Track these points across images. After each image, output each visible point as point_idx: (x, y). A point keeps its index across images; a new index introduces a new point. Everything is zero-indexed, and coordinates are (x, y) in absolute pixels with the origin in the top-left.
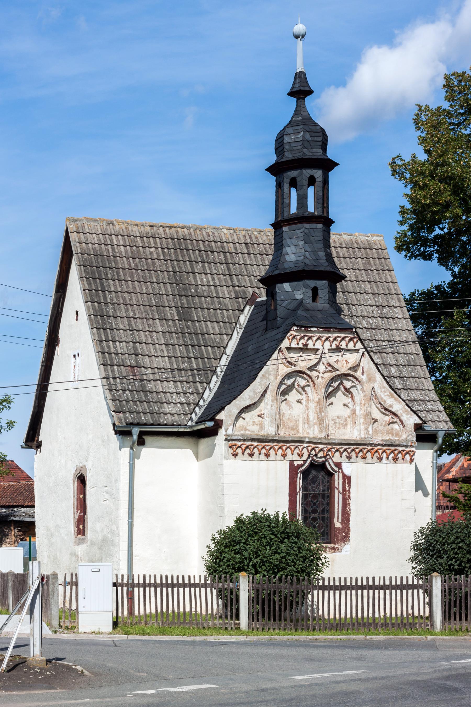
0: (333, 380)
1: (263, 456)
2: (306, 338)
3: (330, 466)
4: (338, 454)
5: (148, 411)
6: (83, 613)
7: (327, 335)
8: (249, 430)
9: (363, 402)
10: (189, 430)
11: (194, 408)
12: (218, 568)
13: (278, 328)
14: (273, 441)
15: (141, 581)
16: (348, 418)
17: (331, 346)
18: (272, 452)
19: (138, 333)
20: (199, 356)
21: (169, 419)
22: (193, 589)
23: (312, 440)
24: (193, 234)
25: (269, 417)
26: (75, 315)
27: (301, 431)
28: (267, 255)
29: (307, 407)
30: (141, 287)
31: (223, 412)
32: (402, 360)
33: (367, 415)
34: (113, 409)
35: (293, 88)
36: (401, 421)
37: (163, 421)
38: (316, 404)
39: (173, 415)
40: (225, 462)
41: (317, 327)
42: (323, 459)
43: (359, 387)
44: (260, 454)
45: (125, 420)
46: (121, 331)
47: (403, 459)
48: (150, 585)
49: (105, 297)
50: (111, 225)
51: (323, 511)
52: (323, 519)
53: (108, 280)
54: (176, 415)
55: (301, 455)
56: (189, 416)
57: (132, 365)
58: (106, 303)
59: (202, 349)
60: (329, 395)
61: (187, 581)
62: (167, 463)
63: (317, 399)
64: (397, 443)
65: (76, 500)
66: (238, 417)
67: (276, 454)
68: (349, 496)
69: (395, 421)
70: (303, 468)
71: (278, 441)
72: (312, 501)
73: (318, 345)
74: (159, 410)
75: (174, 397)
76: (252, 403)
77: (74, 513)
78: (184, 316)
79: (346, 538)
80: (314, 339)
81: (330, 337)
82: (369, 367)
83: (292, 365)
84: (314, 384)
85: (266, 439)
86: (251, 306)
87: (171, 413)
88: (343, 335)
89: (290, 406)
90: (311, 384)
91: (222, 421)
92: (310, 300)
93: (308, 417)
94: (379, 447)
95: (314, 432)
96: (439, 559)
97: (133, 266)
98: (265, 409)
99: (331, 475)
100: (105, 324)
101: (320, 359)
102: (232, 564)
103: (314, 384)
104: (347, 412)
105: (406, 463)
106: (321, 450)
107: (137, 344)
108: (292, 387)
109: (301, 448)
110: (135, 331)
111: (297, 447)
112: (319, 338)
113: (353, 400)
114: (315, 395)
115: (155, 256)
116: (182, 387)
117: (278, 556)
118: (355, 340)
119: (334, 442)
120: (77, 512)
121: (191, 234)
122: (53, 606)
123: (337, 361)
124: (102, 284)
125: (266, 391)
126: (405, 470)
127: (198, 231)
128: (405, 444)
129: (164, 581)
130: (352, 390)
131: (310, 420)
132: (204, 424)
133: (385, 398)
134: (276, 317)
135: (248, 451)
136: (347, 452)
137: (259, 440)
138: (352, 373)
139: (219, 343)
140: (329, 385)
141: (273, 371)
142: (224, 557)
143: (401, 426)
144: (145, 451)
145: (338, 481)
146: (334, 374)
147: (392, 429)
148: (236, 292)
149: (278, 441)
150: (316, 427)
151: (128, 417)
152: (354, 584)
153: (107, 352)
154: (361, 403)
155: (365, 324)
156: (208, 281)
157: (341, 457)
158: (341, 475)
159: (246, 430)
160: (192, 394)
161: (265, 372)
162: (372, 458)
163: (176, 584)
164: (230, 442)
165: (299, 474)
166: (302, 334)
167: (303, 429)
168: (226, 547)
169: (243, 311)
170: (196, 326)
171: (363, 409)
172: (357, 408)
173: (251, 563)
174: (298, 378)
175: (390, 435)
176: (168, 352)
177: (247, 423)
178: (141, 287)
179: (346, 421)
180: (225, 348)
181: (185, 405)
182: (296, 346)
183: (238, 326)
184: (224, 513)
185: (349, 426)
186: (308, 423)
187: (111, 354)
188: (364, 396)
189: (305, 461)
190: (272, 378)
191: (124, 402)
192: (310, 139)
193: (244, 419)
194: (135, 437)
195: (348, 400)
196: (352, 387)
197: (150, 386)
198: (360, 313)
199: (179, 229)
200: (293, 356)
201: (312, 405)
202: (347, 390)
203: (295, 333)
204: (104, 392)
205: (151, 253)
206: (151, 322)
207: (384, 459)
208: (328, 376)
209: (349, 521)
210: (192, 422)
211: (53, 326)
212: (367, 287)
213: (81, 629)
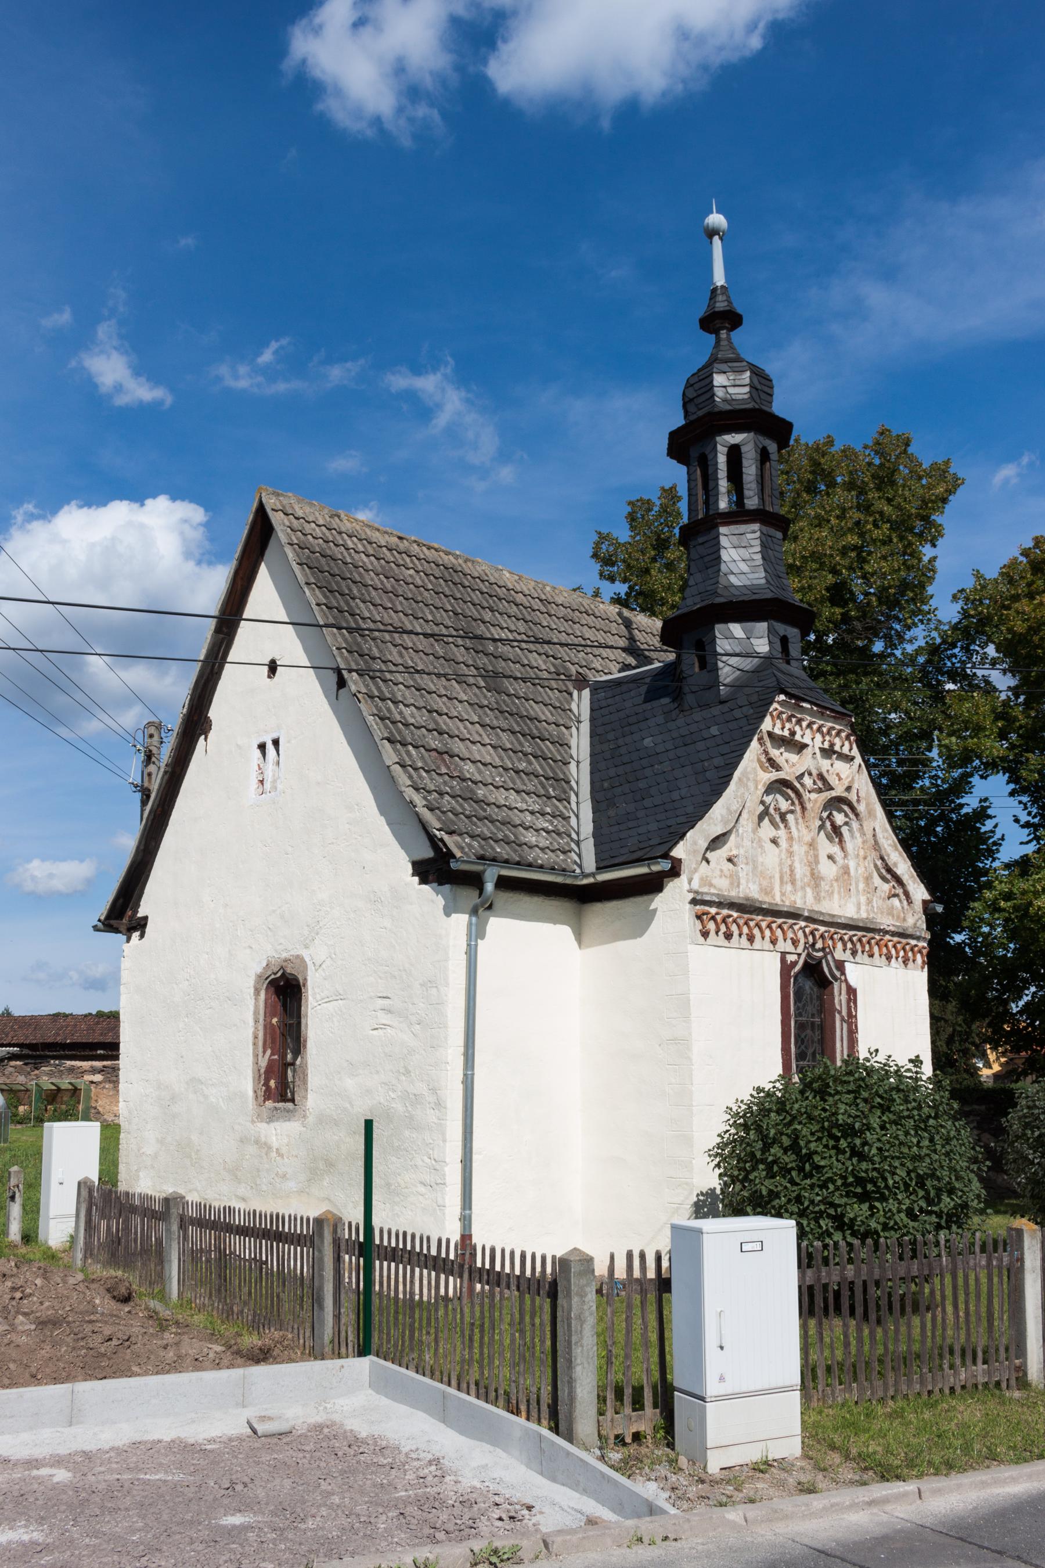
6: (719, 1398)
9: (862, 853)
21: (543, 858)
25: (747, 864)
31: (681, 843)
40: (691, 948)
41: (811, 703)
42: (820, 954)
43: (855, 825)
65: (261, 1028)
68: (856, 1026)
77: (256, 1056)
83: (773, 767)
85: (751, 906)
90: (798, 808)
94: (888, 937)
103: (803, 808)
113: (843, 849)
120: (264, 1052)
122: (578, 1369)
130: (845, 830)
131: (798, 876)
132: (649, 866)
143: (905, 903)
144: (496, 925)
145: (840, 999)
147: (892, 907)
150: (809, 890)
158: (844, 985)
159: (711, 885)
161: (742, 773)
164: (698, 907)
167: (783, 894)
171: (862, 865)
172: (852, 864)
179: (832, 886)
185: (836, 896)
186: (793, 882)
195: (835, 849)
201: (800, 850)
211: (200, 697)
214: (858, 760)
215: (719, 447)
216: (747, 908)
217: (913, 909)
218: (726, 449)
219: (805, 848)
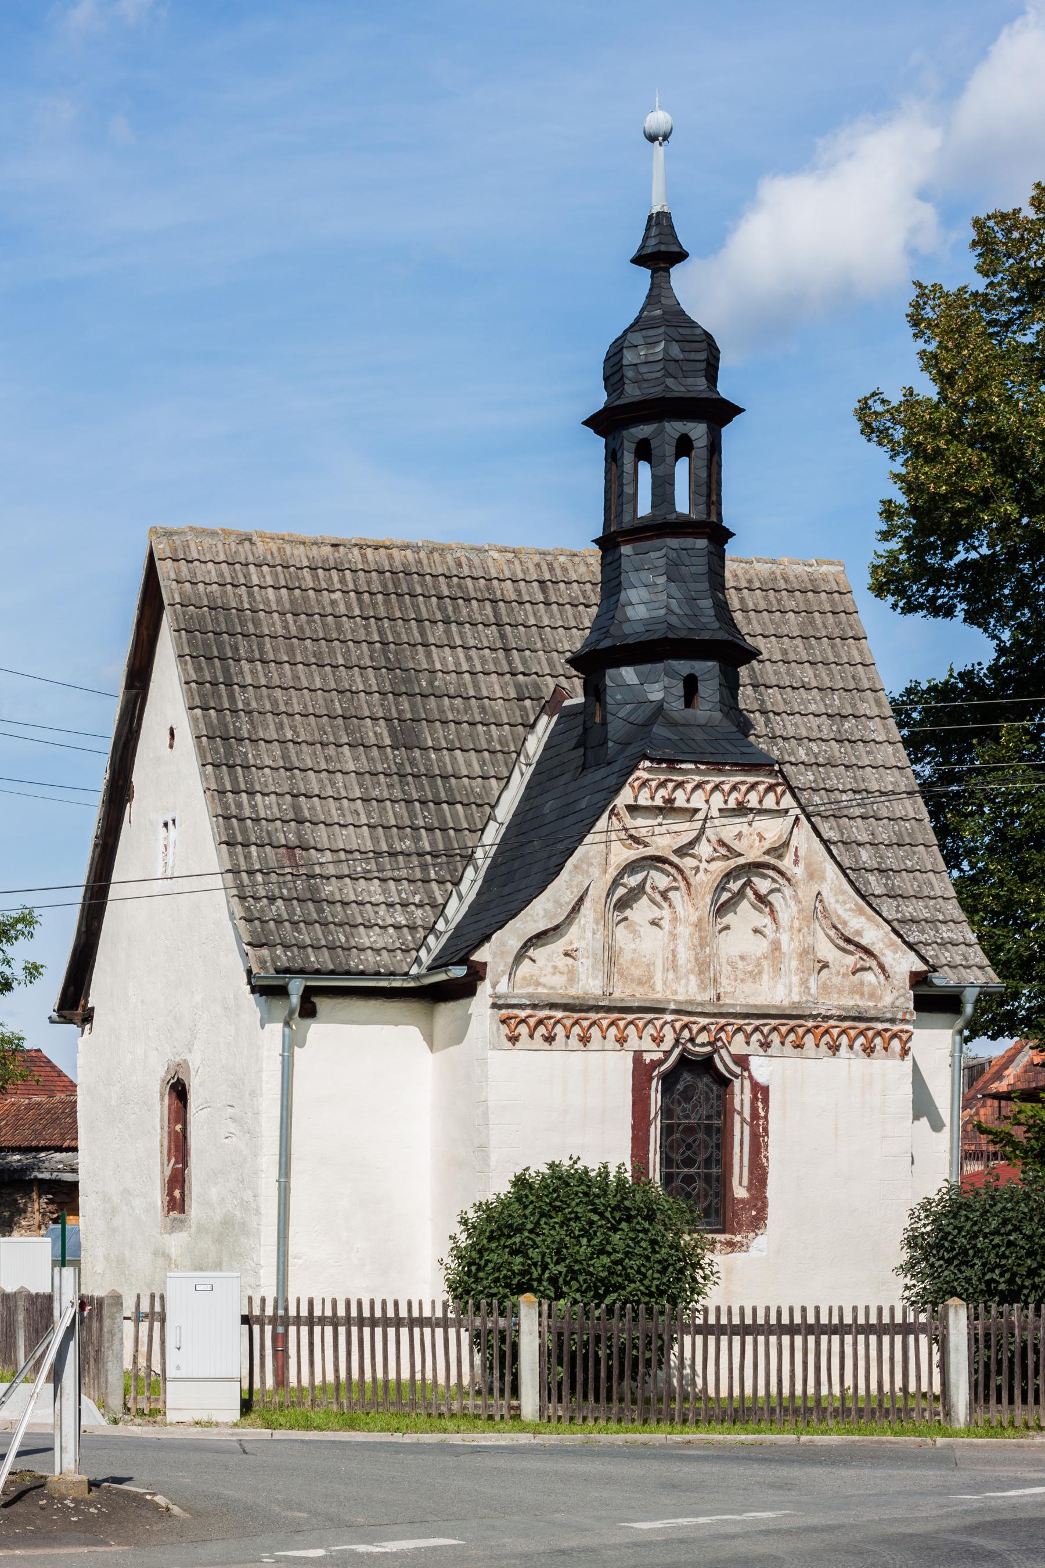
0: (728, 876)
1: (574, 1042)
2: (670, 785)
3: (723, 1062)
4: (740, 1037)
5: (323, 943)
6: (176, 1380)
7: (718, 780)
8: (544, 986)
9: (796, 924)
10: (412, 984)
11: (425, 938)
12: (474, 1286)
13: (609, 764)
14: (597, 1009)
15: (304, 1312)
16: (764, 960)
17: (726, 802)
18: (595, 1032)
19: (303, 774)
20: (436, 825)
22: (417, 1331)
23: (683, 1007)
24: (425, 562)
25: (588, 957)
26: (168, 737)
27: (659, 986)
28: (587, 606)
29: (673, 936)
30: (310, 676)
31: (487, 945)
32: (884, 832)
33: (806, 952)
34: (247, 938)
37: (357, 966)
38: (691, 929)
39: (377, 951)
40: (491, 1054)
41: (695, 762)
42: (709, 1049)
43: (788, 891)
44: (568, 1037)
45: (273, 962)
46: (267, 771)
47: (886, 1049)
48: (323, 1321)
49: (232, 697)
50: (247, 543)
51: (708, 1163)
52: (708, 1178)
53: (239, 661)
54: (384, 953)
55: (658, 1040)
56: (414, 953)
57: (291, 844)
58: (234, 712)
59: (442, 810)
60: (721, 910)
62: (365, 1055)
63: (694, 919)
64: (872, 1013)
66: (520, 956)
67: (605, 1038)
68: (766, 1129)
69: (868, 965)
70: (662, 1068)
71: (609, 1009)
72: (684, 1141)
73: (698, 801)
74: (347, 941)
75: (381, 913)
76: (550, 926)
78: (405, 737)
79: (758, 1222)
80: (689, 787)
81: (723, 783)
82: (809, 849)
83: (639, 843)
84: (688, 884)
85: (581, 1005)
86: (551, 716)
87: (375, 948)
88: (752, 779)
89: (634, 932)
90: (682, 884)
91: (485, 964)
92: (680, 704)
93: (674, 956)
94: (832, 1023)
95: (687, 990)
97: (293, 630)
98: (579, 940)
99: (724, 1083)
100: (232, 755)
101: (702, 830)
102: (505, 1277)
103: (688, 884)
104: (762, 946)
105: (894, 1058)
106: (704, 1028)
107: (302, 799)
109: (658, 1023)
110: (296, 771)
111: (650, 1022)
112: (698, 786)
113: (774, 920)
114: (689, 908)
115: (342, 609)
116: (399, 892)
117: (605, 1260)
118: (779, 789)
119: (731, 1010)
121: (420, 562)
122: (110, 1364)
123: (739, 835)
124: (226, 670)
125: (581, 900)
126: (890, 1074)
127: (436, 555)
128: (889, 1015)
129: (354, 1313)
131: (680, 963)
132: (446, 972)
133: (845, 916)
135: (542, 1030)
136: (762, 1032)
137: (566, 1007)
138: (773, 861)
139: (480, 796)
140: (721, 888)
141: (598, 857)
142: (488, 1262)
143: (882, 977)
145: (741, 1097)
146: (732, 863)
147: (862, 983)
148: (518, 687)
149: (609, 1009)
150: (693, 978)
151: (279, 957)
152: (773, 1321)
153: (235, 817)
154: (792, 927)
155: (802, 754)
156: (457, 663)
157: (748, 1043)
158: (747, 1083)
159: (538, 984)
161: (580, 860)
162: (817, 1046)
163: (379, 1319)
164: (503, 1011)
165: (654, 1082)
166: (662, 778)
167: (665, 983)
168: (491, 1239)
169: (533, 726)
170: (429, 759)
171: (796, 939)
172: (784, 938)
173: (547, 1275)
174: (653, 873)
175: (857, 997)
176: (369, 816)
177: (541, 969)
178: (310, 676)
179: (759, 964)
180: (493, 807)
181: (405, 930)
182: (649, 803)
183: (522, 759)
184: (488, 1165)
185: (765, 976)
186: (675, 969)
187: (244, 820)
188: (799, 912)
189: (668, 1054)
190: (595, 871)
191: (272, 923)
193: (534, 961)
194: (295, 999)
195: (763, 920)
196: (772, 891)
197: (328, 889)
198: (791, 731)
199: (395, 552)
200: (641, 824)
201: (684, 931)
202: (762, 899)
203: (645, 775)
204: (228, 902)
205: (333, 603)
206: (331, 750)
207: (844, 1049)
208: (720, 867)
209: (765, 1184)
210: (418, 966)
211: (121, 760)
212: (808, 675)
213: (171, 1416)
215: (626, 444)
217: (891, 984)
218: (634, 446)
219: (691, 929)
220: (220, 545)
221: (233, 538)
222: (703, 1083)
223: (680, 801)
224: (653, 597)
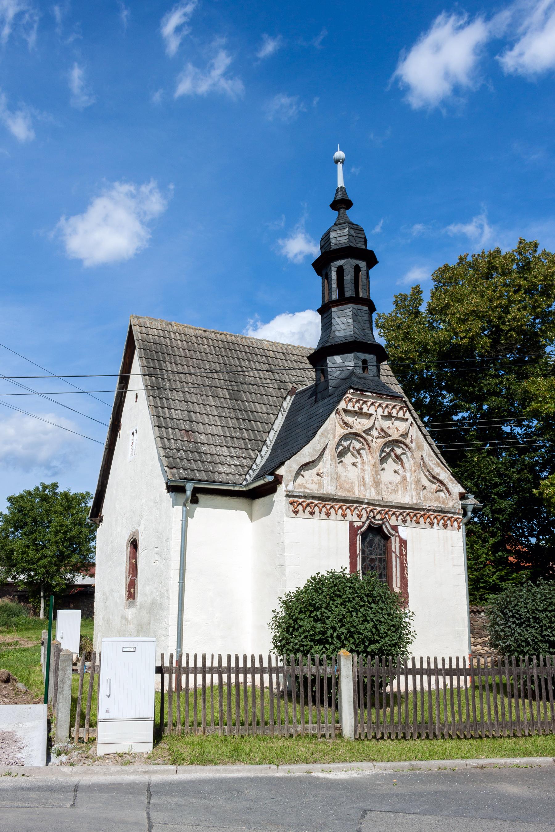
0: (386, 445)
1: (323, 516)
2: (361, 402)
4: (394, 517)
5: (202, 469)
6: (105, 720)
7: (380, 402)
8: (308, 489)
9: (413, 469)
10: (244, 489)
11: (248, 471)
12: (292, 640)
13: (330, 396)
14: (334, 500)
15: (199, 664)
17: (383, 412)
18: (332, 511)
19: (192, 404)
20: (250, 428)
21: (224, 478)
23: (371, 502)
24: (240, 341)
25: (328, 476)
26: (135, 398)
28: (301, 363)
29: (363, 470)
33: (418, 481)
34: (166, 464)
35: (335, 198)
36: (447, 490)
37: (218, 479)
38: (371, 467)
39: (227, 474)
40: (286, 519)
41: (372, 392)
42: (380, 522)
43: (409, 454)
44: (320, 513)
45: (179, 475)
46: (177, 401)
47: (452, 526)
50: (170, 326)
53: (165, 362)
54: (230, 475)
56: (244, 476)
57: (187, 429)
59: (252, 423)
60: (383, 460)
61: (266, 664)
63: (372, 462)
64: (446, 510)
67: (337, 514)
68: (406, 560)
69: (441, 489)
70: (362, 530)
72: (370, 565)
73: (372, 410)
74: (213, 469)
75: (228, 460)
76: (311, 460)
78: (235, 396)
80: (369, 404)
81: (382, 403)
82: (417, 436)
83: (348, 427)
84: (369, 447)
85: (326, 498)
86: (292, 396)
87: (227, 473)
88: (394, 404)
89: (345, 468)
90: (366, 447)
91: (282, 476)
92: (361, 371)
93: (364, 479)
94: (431, 513)
95: (370, 494)
96: (528, 628)
98: (323, 468)
99: (386, 538)
100: (161, 394)
102: (311, 635)
103: (369, 447)
104: (397, 479)
105: (454, 530)
106: (379, 512)
107: (192, 413)
108: (346, 450)
109: (360, 508)
110: (189, 403)
111: (356, 508)
112: (372, 404)
113: (403, 467)
114: (370, 458)
115: (208, 351)
116: (236, 453)
118: (405, 409)
119: (391, 504)
121: (238, 341)
122: (60, 705)
125: (324, 450)
127: (243, 340)
128: (453, 511)
129: (233, 665)
130: (403, 457)
131: (367, 482)
133: (433, 466)
134: (328, 387)
135: (308, 509)
136: (403, 516)
137: (320, 498)
138: (403, 440)
139: (267, 420)
141: (332, 428)
142: (300, 626)
143: (447, 494)
145: (395, 545)
146: (387, 439)
147: (439, 497)
150: (373, 489)
151: (181, 473)
153: (162, 417)
154: (411, 470)
157: (397, 520)
158: (397, 539)
159: (305, 488)
160: (245, 458)
162: (425, 523)
163: (250, 668)
164: (291, 499)
165: (359, 536)
166: (358, 398)
167: (359, 492)
168: (301, 612)
169: (285, 398)
170: (245, 405)
172: (408, 475)
173: (335, 634)
174: (354, 441)
175: (438, 503)
176: (221, 422)
177: (307, 481)
179: (397, 486)
180: (272, 425)
181: (239, 467)
182: (352, 409)
183: (282, 409)
184: (285, 575)
185: (400, 492)
187: (166, 418)
188: (414, 463)
189: (364, 523)
190: (330, 437)
191: (178, 459)
192: (355, 235)
193: (303, 477)
194: (189, 493)
195: (399, 467)
196: (402, 454)
197: (203, 449)
199: (228, 336)
201: (368, 468)
202: (398, 457)
203: (351, 396)
204: (158, 450)
205: (204, 349)
207: (435, 525)
209: (407, 586)
210: (249, 481)
213: (101, 750)
214: (411, 420)
216: (324, 499)
217: (452, 498)
220: (159, 324)
221: (164, 323)
222: (377, 539)
223: (365, 410)
224: (347, 327)
